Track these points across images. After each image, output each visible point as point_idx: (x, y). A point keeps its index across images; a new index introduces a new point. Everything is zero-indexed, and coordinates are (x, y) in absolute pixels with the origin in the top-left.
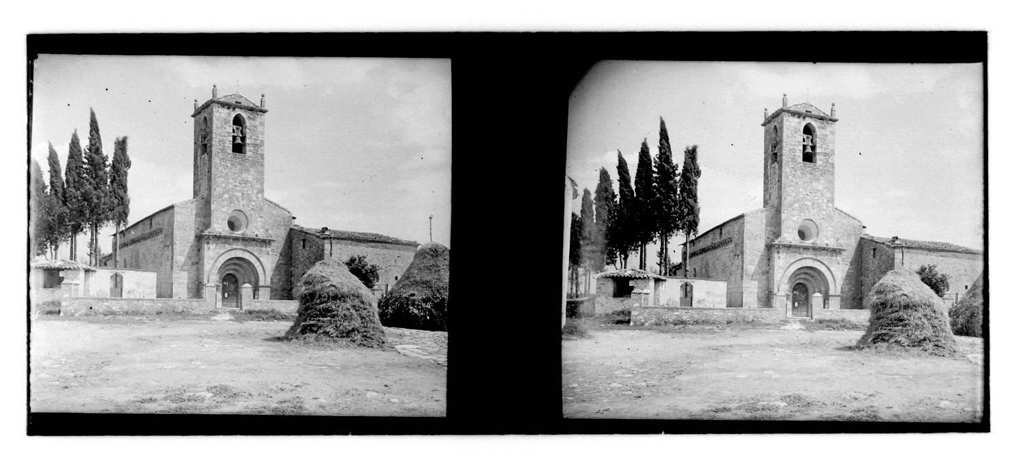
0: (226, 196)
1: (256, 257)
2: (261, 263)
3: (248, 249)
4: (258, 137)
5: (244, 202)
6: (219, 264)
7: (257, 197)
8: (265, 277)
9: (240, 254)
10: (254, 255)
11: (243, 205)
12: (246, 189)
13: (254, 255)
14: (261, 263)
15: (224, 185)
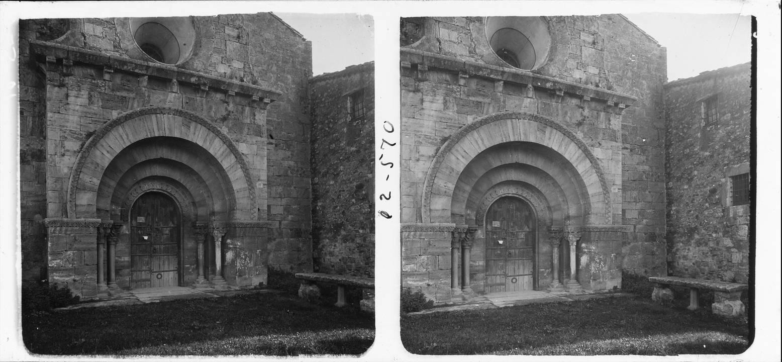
9: (172, 127)
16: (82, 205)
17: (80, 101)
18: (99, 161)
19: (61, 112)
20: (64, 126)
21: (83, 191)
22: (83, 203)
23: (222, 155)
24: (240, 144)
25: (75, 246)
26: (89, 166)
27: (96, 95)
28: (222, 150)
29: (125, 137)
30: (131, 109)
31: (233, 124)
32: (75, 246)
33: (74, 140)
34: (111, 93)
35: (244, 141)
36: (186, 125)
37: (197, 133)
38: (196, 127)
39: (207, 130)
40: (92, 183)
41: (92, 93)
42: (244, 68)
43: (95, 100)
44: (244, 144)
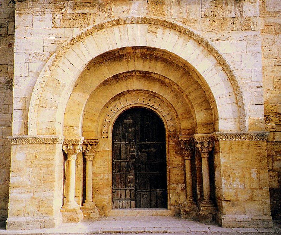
10: (190, 35)
13: (190, 35)
17: (42, 24)
19: (26, 37)
20: (28, 50)
21: (45, 108)
25: (36, 162)
26: (51, 84)
27: (58, 16)
29: (86, 53)
31: (211, 21)
33: (38, 61)
34: (73, 12)
36: (152, 31)
39: (178, 33)
40: (53, 100)
41: (55, 15)
43: (58, 22)
44: (227, 42)
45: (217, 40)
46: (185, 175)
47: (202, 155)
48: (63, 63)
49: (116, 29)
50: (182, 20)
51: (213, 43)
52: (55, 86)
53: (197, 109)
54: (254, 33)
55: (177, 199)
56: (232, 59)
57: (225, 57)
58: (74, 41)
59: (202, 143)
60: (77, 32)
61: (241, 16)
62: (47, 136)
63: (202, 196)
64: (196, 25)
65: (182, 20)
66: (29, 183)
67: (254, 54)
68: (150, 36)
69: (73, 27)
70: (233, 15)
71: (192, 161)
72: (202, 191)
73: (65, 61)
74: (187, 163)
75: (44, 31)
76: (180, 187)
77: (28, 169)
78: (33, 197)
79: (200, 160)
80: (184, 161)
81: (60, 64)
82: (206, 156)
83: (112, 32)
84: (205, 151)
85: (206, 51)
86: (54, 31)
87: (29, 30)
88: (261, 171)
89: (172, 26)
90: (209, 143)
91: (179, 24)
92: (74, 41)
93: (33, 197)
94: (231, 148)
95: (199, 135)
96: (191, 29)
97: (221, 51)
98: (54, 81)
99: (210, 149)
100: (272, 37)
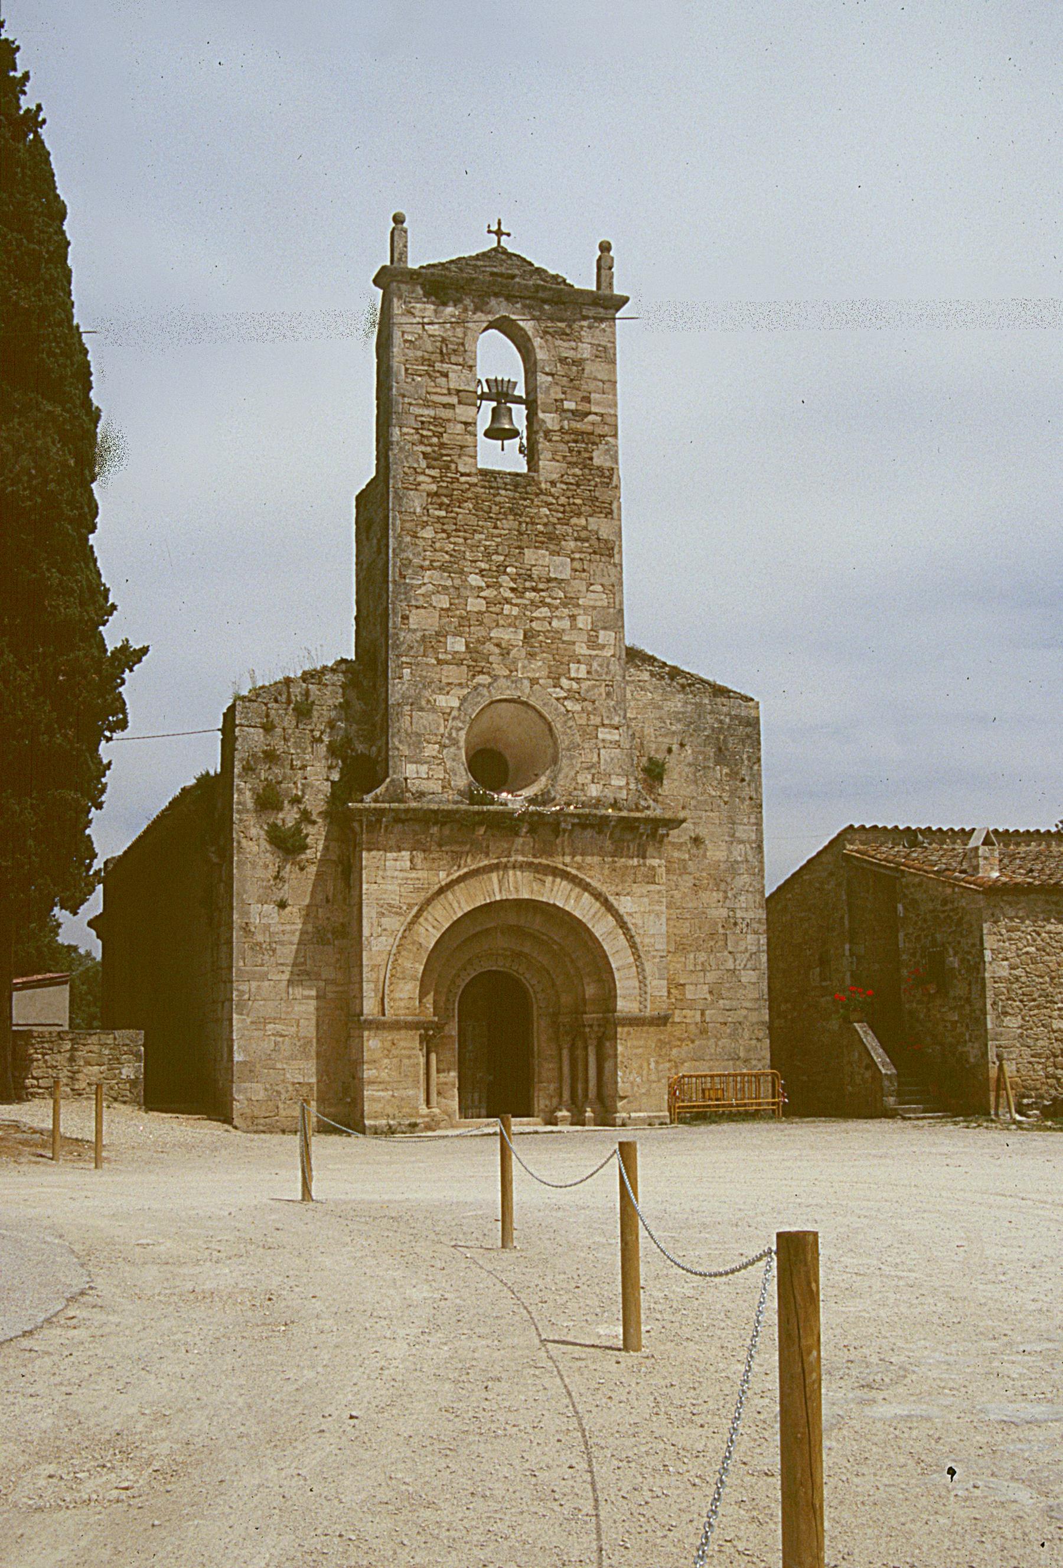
0: (457, 645)
1: (598, 896)
2: (622, 924)
3: (558, 862)
4: (587, 400)
5: (538, 668)
6: (429, 934)
7: (593, 643)
8: (643, 982)
10: (586, 887)
11: (534, 681)
12: (544, 611)
13: (586, 887)
14: (622, 924)
15: (443, 601)
16: (401, 999)
18: (422, 940)
22: (402, 996)
23: (594, 916)
24: (622, 898)
25: (394, 1052)
28: (593, 911)
29: (455, 905)
30: (465, 866)
32: (394, 1052)
35: (628, 894)
37: (555, 889)
38: (554, 881)
42: (628, 784)
43: (418, 861)
44: (629, 898)
45: (617, 894)
46: (561, 1068)
47: (590, 1041)
48: (426, 919)
49: (494, 876)
50: (575, 865)
51: (611, 899)
52: (415, 949)
53: (586, 980)
54: (658, 887)
55: (547, 1102)
56: (634, 921)
57: (626, 918)
58: (441, 891)
59: (591, 1026)
60: (443, 878)
61: (645, 865)
62: (410, 1018)
63: (586, 1096)
64: (592, 873)
65: (575, 865)
66: (388, 1079)
67: (658, 915)
68: (536, 886)
69: (438, 869)
70: (636, 863)
71: (572, 1049)
72: (586, 1090)
73: (430, 918)
74: (565, 1052)
75: (401, 875)
76: (552, 1086)
77: (386, 1061)
78: (393, 1096)
79: (586, 1048)
80: (560, 1049)
81: (421, 920)
82: (595, 1042)
83: (490, 879)
84: (593, 1036)
85: (603, 908)
86: (414, 875)
87: (381, 873)
88: (661, 1061)
89: (565, 875)
90: (599, 1025)
91: (574, 872)
92: (441, 891)
93: (393, 1096)
94: (629, 1033)
95: (588, 1016)
96: (588, 880)
97: (622, 911)
98: (414, 943)
99: (600, 1035)
100: (675, 878)
